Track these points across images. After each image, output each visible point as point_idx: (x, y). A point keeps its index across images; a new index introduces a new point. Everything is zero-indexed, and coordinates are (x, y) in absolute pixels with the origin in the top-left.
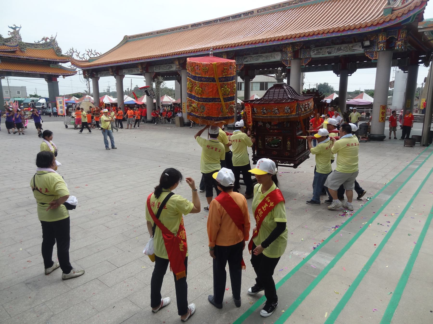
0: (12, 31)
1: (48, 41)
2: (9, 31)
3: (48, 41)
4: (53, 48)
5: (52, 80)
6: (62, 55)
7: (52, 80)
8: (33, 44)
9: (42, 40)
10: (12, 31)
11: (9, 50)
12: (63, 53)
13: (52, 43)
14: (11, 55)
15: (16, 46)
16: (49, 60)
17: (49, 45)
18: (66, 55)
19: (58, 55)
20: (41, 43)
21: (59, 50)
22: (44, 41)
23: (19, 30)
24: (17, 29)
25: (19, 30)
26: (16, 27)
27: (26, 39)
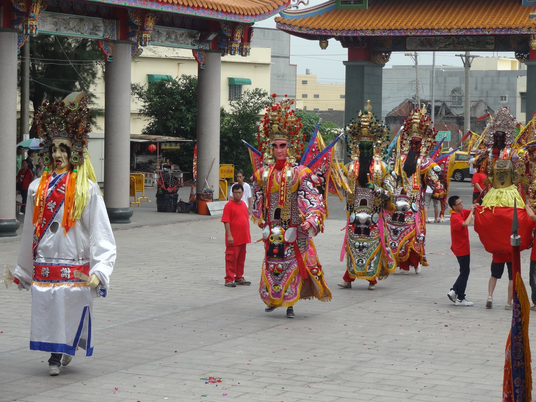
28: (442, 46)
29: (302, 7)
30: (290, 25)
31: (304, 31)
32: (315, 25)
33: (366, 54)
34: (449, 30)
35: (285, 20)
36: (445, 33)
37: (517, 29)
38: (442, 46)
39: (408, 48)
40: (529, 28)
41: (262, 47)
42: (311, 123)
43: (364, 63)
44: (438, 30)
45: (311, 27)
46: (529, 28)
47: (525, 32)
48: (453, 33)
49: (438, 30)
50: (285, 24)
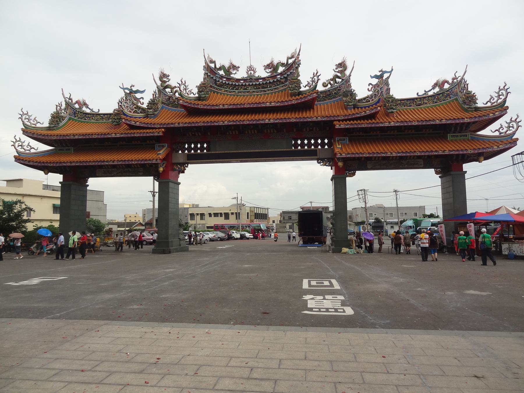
0: (375, 81)
1: (446, 86)
2: (370, 84)
3: (446, 86)
4: (456, 100)
5: (450, 170)
6: (477, 109)
7: (450, 170)
8: (413, 99)
9: (434, 88)
10: (375, 81)
11: (363, 114)
12: (482, 101)
13: (456, 90)
14: (365, 124)
15: (376, 104)
16: (444, 122)
17: (448, 95)
18: (489, 104)
19: (466, 110)
20: (431, 93)
21: (471, 98)
22: (437, 90)
23: (388, 78)
24: (386, 76)
25: (388, 78)
26: (383, 72)
27: (400, 90)
28: (115, 173)
29: (33, 151)
30: (23, 160)
31: (31, 164)
32: (38, 160)
33: (75, 179)
34: (113, 161)
35: (21, 157)
36: (111, 163)
37: (150, 160)
38: (115, 173)
39: (97, 175)
40: (157, 160)
41: (31, 180)
42: (95, 223)
43: (71, 183)
44: (107, 161)
45: (35, 161)
46: (157, 160)
47: (154, 162)
48: (116, 163)
49: (107, 161)
50: (20, 159)
